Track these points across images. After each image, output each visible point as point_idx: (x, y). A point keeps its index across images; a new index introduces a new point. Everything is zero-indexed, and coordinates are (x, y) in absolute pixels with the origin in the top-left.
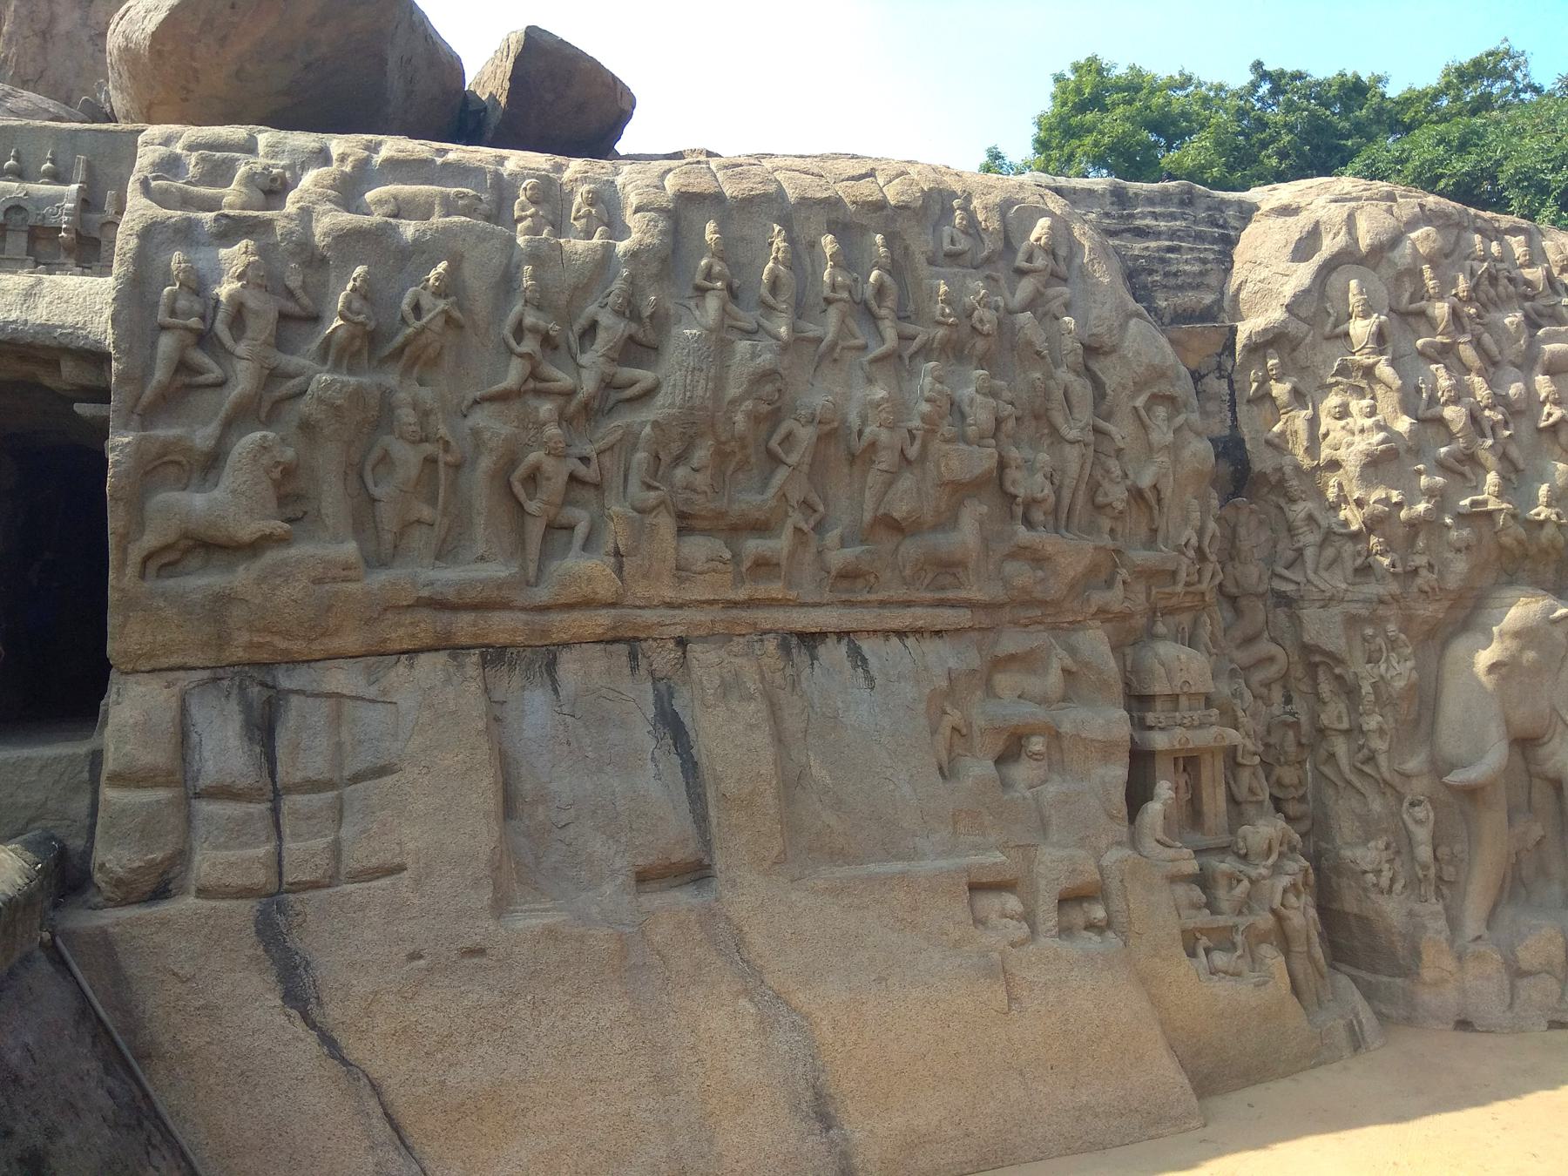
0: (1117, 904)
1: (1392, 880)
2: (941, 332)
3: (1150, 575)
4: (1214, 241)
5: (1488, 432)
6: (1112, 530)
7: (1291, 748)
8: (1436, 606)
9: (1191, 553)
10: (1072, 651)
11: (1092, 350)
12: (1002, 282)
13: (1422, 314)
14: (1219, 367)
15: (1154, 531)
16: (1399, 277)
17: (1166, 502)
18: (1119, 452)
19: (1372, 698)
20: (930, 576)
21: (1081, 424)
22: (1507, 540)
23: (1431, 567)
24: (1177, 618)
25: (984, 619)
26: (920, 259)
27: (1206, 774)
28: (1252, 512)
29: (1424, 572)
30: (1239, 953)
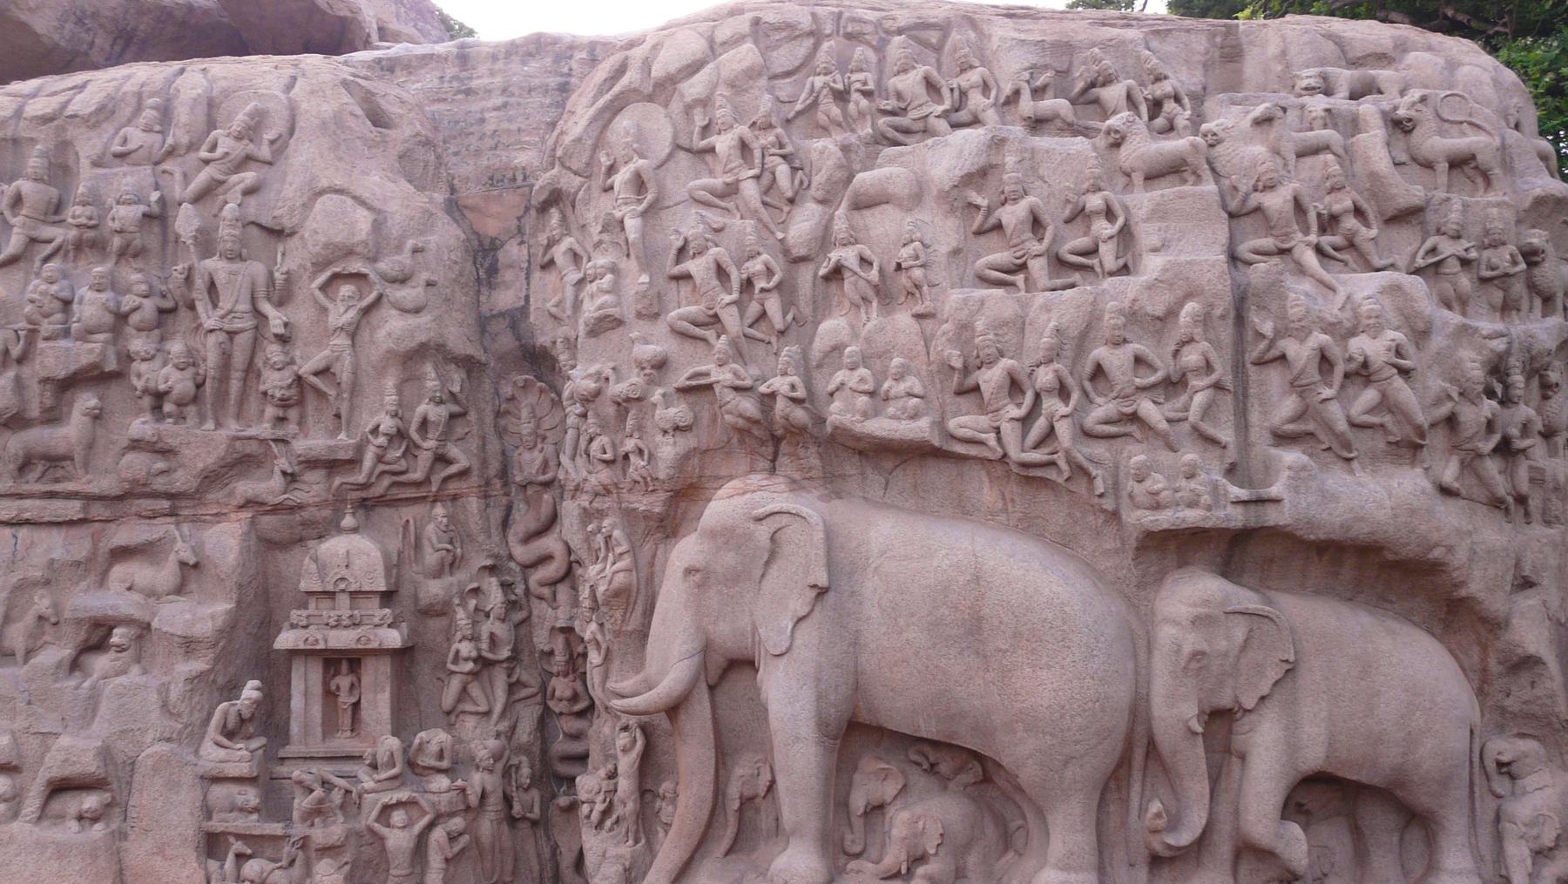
1: (606, 813)
2: (73, 234)
3: (332, 465)
5: (735, 285)
6: (281, 420)
7: (560, 658)
8: (652, 498)
9: (382, 440)
11: (277, 233)
13: (711, 150)
14: (520, 230)
15: (338, 416)
16: (688, 109)
17: (344, 386)
18: (283, 340)
19: (587, 603)
20: (40, 468)
21: (222, 312)
23: (641, 452)
25: (98, 511)
26: (85, 163)
27: (367, 679)
28: (541, 391)
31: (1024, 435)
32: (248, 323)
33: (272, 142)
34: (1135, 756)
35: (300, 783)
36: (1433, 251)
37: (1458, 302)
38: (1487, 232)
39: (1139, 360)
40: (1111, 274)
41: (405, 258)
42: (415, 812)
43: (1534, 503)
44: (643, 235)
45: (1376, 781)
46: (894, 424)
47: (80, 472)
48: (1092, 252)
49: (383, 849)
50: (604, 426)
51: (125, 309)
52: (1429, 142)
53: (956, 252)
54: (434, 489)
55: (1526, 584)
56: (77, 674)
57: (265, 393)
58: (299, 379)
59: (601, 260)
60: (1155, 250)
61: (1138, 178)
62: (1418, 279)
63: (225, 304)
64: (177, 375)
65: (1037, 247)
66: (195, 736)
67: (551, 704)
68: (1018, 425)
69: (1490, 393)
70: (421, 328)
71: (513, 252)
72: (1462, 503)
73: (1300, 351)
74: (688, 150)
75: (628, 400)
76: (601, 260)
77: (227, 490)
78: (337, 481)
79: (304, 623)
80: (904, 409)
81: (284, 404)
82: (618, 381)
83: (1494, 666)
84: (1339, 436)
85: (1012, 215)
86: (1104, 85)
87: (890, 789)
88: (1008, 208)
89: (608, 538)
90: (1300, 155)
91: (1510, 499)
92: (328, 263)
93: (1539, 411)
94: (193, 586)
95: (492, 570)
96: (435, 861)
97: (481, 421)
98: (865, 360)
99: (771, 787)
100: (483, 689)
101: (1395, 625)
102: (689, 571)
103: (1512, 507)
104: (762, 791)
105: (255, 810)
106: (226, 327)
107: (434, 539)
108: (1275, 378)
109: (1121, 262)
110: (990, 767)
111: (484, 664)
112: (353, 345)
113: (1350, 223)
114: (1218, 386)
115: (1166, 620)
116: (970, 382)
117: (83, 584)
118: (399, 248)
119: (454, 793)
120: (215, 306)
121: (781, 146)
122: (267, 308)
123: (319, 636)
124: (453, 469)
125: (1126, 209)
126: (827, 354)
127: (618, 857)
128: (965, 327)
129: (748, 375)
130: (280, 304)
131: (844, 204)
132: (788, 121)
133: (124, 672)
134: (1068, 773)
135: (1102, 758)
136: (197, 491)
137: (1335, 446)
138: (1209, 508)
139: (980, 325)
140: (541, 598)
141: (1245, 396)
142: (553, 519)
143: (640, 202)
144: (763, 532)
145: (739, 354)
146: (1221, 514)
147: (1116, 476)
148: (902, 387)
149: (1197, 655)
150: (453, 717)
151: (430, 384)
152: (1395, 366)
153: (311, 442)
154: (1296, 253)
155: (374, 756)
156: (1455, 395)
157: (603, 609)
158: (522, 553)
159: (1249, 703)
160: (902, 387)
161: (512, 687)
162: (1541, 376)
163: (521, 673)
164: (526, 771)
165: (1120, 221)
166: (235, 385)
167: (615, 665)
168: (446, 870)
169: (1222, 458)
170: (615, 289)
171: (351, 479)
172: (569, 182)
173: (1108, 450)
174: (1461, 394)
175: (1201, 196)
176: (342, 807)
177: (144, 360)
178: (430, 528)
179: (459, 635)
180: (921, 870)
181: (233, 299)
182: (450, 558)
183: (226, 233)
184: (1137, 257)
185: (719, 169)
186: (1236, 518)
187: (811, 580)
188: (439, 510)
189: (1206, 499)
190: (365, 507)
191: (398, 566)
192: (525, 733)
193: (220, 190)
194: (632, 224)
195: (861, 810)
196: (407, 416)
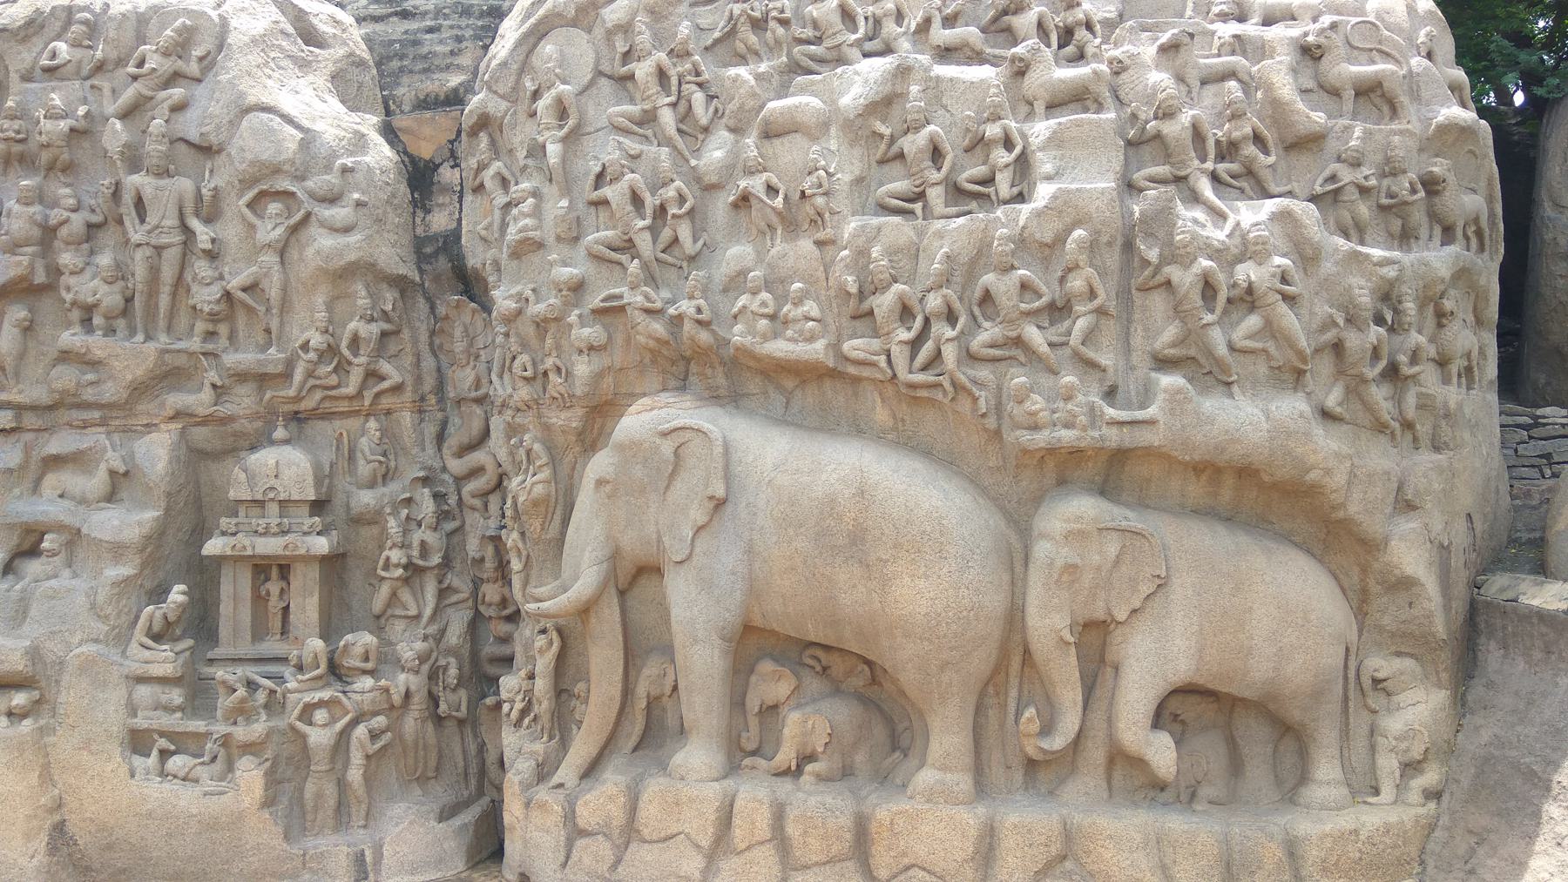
0: (62, 698)
1: (524, 712)
3: (262, 379)
4: (482, 15)
5: (649, 211)
6: (211, 335)
7: (490, 564)
9: (312, 355)
10: (132, 455)
11: (206, 150)
12: (107, 92)
13: (631, 77)
14: (453, 154)
15: (268, 331)
16: (610, 34)
21: (147, 227)
22: (642, 339)
23: (559, 370)
24: (337, 423)
25: (30, 420)
27: (296, 581)
29: (552, 376)
30: (206, 759)
31: (912, 358)
32: (178, 238)
33: (201, 59)
34: (1011, 663)
35: (224, 682)
36: (1333, 178)
37: (1355, 230)
38: (1388, 160)
39: (1025, 286)
40: (1006, 202)
41: (333, 179)
42: (337, 711)
43: (1423, 429)
44: (564, 160)
45: (1247, 694)
46: (791, 346)
47: (12, 382)
48: (989, 181)
49: (305, 747)
50: (525, 346)
51: (53, 222)
52: (1336, 70)
53: (859, 181)
54: (367, 403)
55: (1406, 505)
56: (10, 577)
57: (194, 308)
58: (227, 295)
59: (525, 185)
60: (1049, 178)
61: (1040, 107)
62: (1312, 206)
63: (152, 219)
64: (106, 287)
65: (935, 176)
66: (121, 638)
67: (482, 608)
68: (907, 350)
69: (1379, 320)
70: (352, 246)
71: (447, 174)
72: (1345, 427)
73: (1185, 278)
74: (610, 77)
75: (546, 320)
76: (525, 185)
77: (157, 401)
78: (268, 395)
79: (234, 529)
80: (801, 332)
81: (214, 318)
82: (537, 302)
83: (1375, 588)
84: (1218, 362)
85: (914, 144)
86: (1015, 13)
87: (781, 689)
88: (910, 137)
89: (529, 452)
90: (1204, 83)
91: (1396, 425)
92: (256, 181)
93: (1432, 340)
94: (124, 495)
95: (425, 481)
96: (357, 758)
97: (415, 341)
98: (768, 285)
99: (675, 688)
100: (414, 595)
101: (1273, 545)
102: (600, 483)
103: (1398, 432)
104: (668, 690)
105: (181, 708)
106: (154, 241)
107: (367, 450)
108: (1158, 303)
109: (1015, 190)
110: (879, 672)
111: (413, 571)
112: (282, 263)
113: (1251, 150)
114: (1101, 312)
115: (1042, 536)
116: (866, 306)
117: (17, 491)
118: (328, 168)
119: (377, 693)
120: (142, 221)
121: (698, 74)
122: (195, 224)
123: (247, 542)
124: (386, 385)
125: (1024, 136)
126: (732, 279)
127: (532, 753)
128: (862, 253)
129: (659, 298)
130: (208, 221)
131: (755, 133)
132: (706, 49)
133: (56, 576)
134: (945, 679)
135: (980, 662)
136: (127, 402)
137: (1215, 370)
138: (1084, 429)
139: (875, 252)
140: (473, 509)
141: (1130, 321)
142: (486, 433)
143: (561, 127)
144: (667, 447)
145: (651, 279)
146: (1096, 434)
147: (999, 396)
148: (800, 311)
149: (1071, 568)
150: (383, 621)
151: (360, 302)
152: (1279, 292)
153: (240, 356)
154: (1192, 180)
155: (300, 658)
156: (1341, 322)
157: (524, 518)
158: (456, 466)
159: (1121, 615)
160: (800, 311)
161: (443, 593)
162: (1436, 304)
163: (452, 579)
164: (453, 672)
165: (1018, 150)
166: (164, 300)
167: (534, 572)
168: (367, 767)
169: (1101, 380)
170: (537, 212)
171: (282, 393)
172: (497, 107)
173: (993, 372)
174: (1348, 321)
175: (1098, 124)
176: (266, 706)
177: (72, 273)
178: (364, 440)
179: (389, 543)
180: (809, 768)
181: (160, 214)
182: (383, 470)
183: (154, 148)
184: (1032, 187)
185: (638, 96)
186: (1113, 437)
187: (710, 492)
188: (372, 424)
189: (1083, 419)
190: (299, 420)
191: (331, 476)
192: (454, 636)
193: (148, 105)
194: (553, 150)
195: (756, 709)
196: (338, 331)
